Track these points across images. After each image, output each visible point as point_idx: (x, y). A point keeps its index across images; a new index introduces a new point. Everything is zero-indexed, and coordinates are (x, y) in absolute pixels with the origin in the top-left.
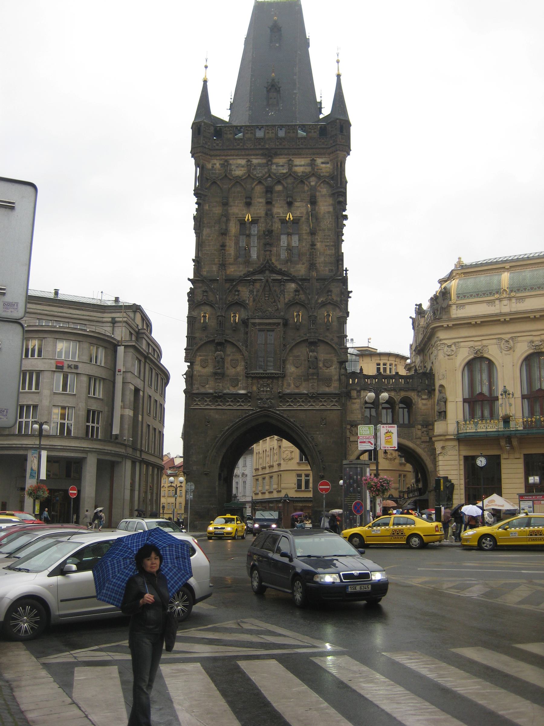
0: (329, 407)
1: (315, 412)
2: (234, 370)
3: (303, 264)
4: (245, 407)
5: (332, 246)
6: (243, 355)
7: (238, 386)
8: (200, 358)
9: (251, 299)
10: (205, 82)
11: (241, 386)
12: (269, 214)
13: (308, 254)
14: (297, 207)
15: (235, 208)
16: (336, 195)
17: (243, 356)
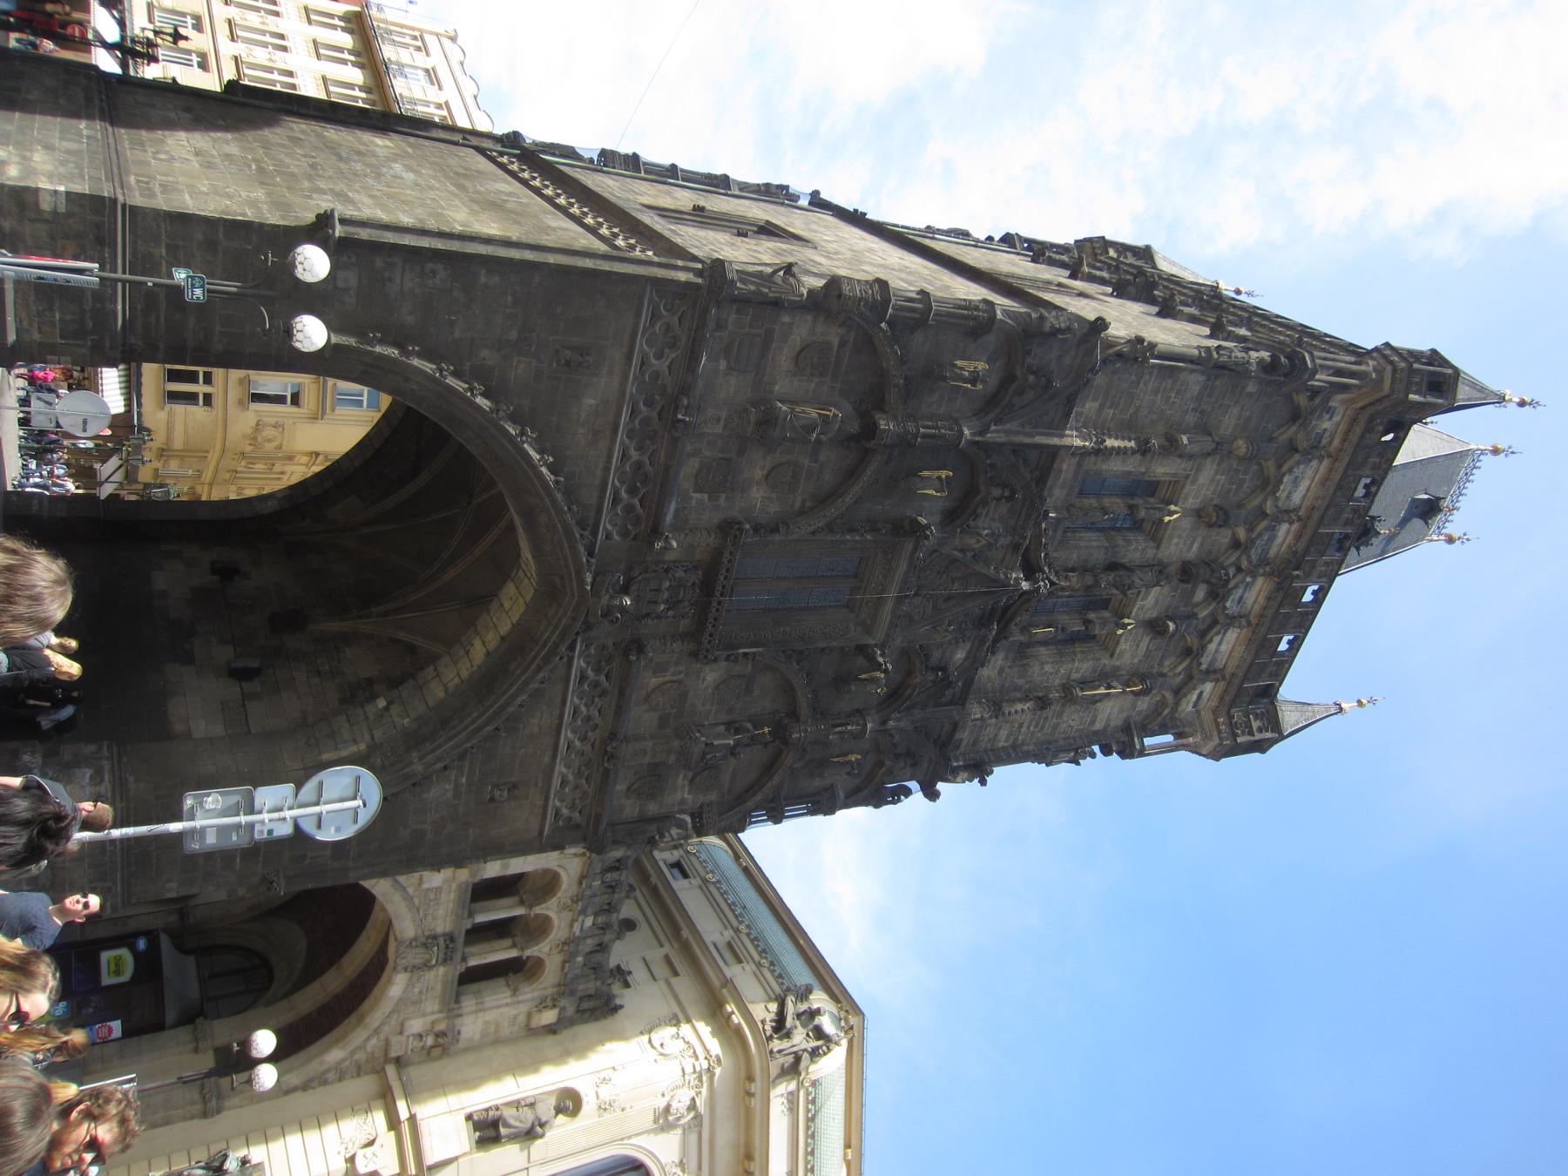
0: (554, 802)
1: (546, 759)
2: (759, 474)
3: (1001, 671)
4: (605, 524)
5: (1016, 739)
6: (802, 512)
7: (694, 492)
8: (836, 342)
9: (973, 541)
10: (1501, 400)
11: (694, 503)
12: (1160, 571)
13: (1021, 682)
14: (1140, 641)
15: (1212, 472)
16: (1124, 738)
17: (798, 505)
